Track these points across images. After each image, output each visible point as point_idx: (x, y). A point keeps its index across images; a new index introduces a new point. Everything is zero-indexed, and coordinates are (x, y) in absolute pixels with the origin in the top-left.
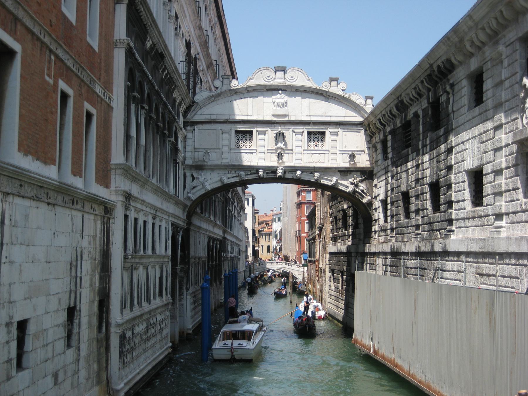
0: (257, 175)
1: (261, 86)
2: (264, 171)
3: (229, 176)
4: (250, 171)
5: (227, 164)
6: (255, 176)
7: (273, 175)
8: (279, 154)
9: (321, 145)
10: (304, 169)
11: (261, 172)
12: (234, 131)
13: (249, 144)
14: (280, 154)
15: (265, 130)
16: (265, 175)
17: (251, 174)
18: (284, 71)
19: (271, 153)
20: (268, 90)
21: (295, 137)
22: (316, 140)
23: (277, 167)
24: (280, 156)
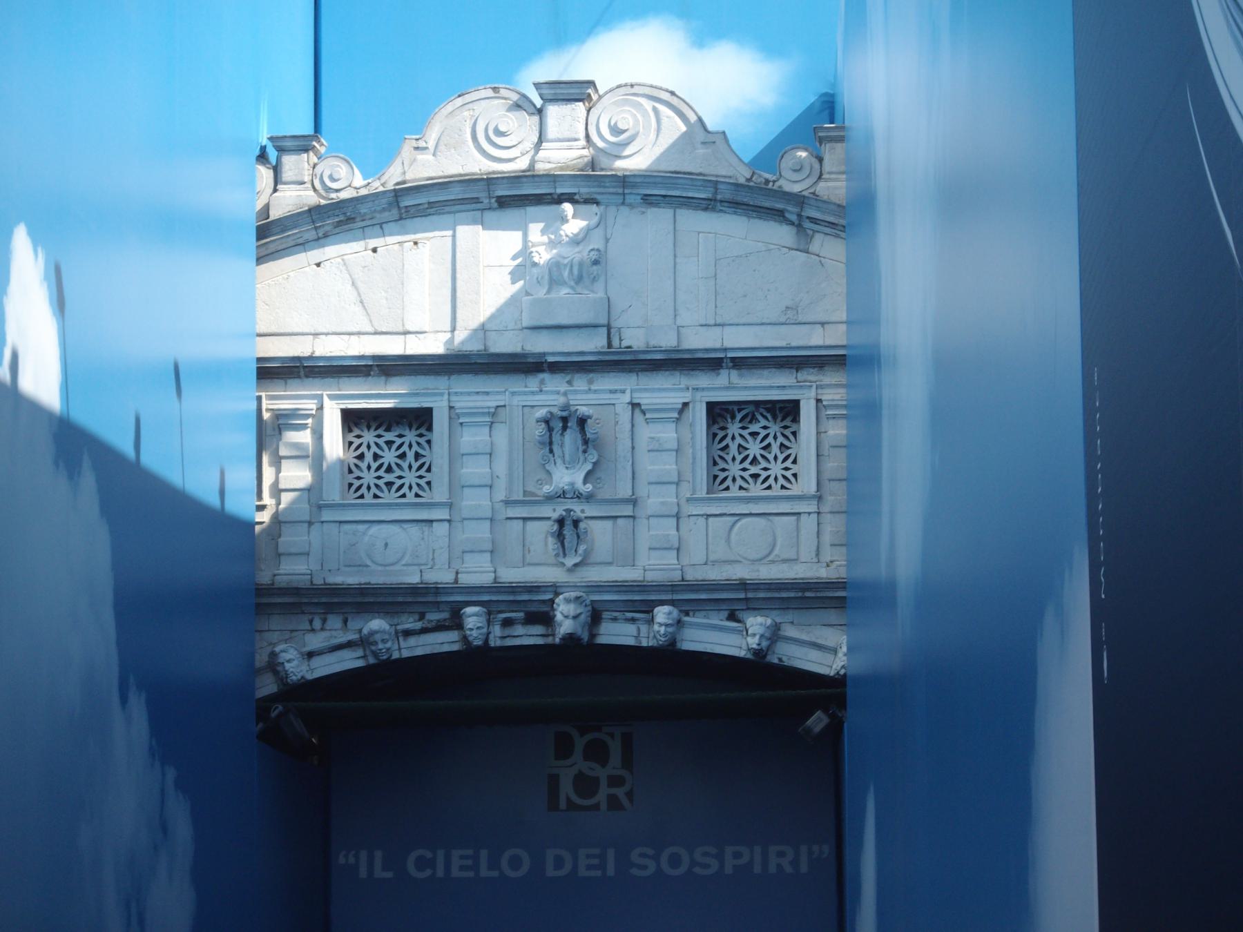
0: (453, 635)
1: (468, 182)
2: (489, 613)
3: (315, 641)
4: (422, 616)
5: (303, 582)
7: (539, 629)
8: (561, 522)
9: (780, 473)
13: (414, 481)
14: (568, 522)
15: (491, 402)
16: (497, 630)
19: (525, 519)
20: (504, 203)
22: (754, 448)
23: (556, 589)
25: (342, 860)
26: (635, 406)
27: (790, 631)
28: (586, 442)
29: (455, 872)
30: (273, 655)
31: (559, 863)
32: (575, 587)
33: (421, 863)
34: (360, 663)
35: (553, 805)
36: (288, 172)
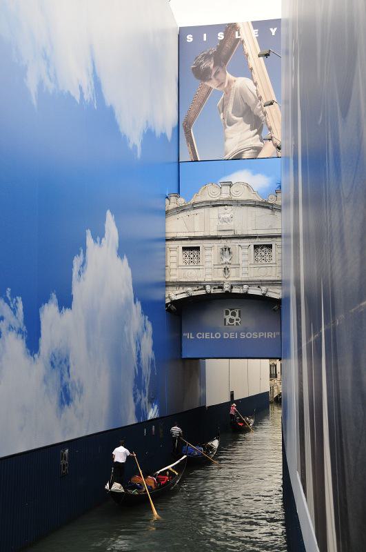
0: (204, 291)
3: (177, 292)
6: (203, 292)
10: (251, 283)
11: (208, 288)
15: (211, 245)
18: (230, 186)
20: (214, 206)
21: (241, 251)
27: (270, 290)
31: (226, 335)
33: (200, 335)
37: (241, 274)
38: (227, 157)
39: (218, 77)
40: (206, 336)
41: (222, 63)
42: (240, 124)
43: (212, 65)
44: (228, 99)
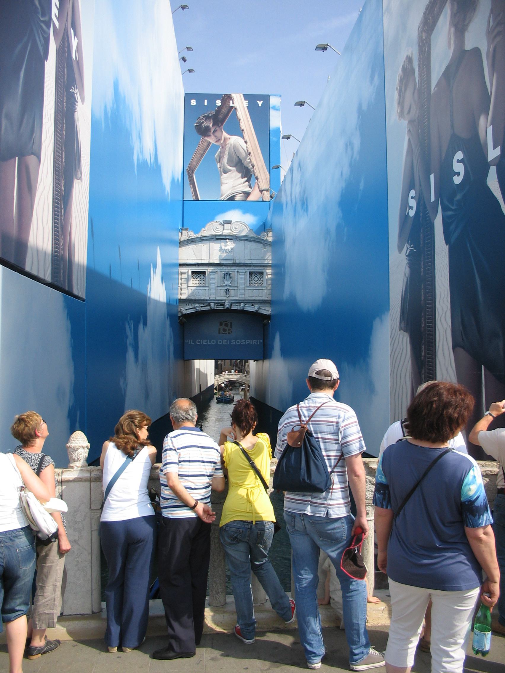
0: (209, 307)
3: (187, 308)
4: (204, 304)
6: (207, 308)
8: (226, 290)
10: (247, 302)
11: (212, 305)
12: (191, 272)
14: (227, 290)
16: (216, 306)
17: (204, 306)
20: (217, 239)
21: (239, 276)
23: (225, 300)
24: (227, 291)
25: (186, 341)
26: (238, 272)
27: (261, 308)
28: (230, 277)
29: (204, 344)
30: (181, 310)
31: (220, 342)
32: (228, 300)
33: (198, 342)
34: (194, 311)
35: (219, 333)
36: (183, 234)
37: (239, 293)
38: (222, 198)
39: (216, 134)
40: (204, 342)
41: (220, 124)
42: (233, 172)
43: (212, 124)
44: (224, 152)
